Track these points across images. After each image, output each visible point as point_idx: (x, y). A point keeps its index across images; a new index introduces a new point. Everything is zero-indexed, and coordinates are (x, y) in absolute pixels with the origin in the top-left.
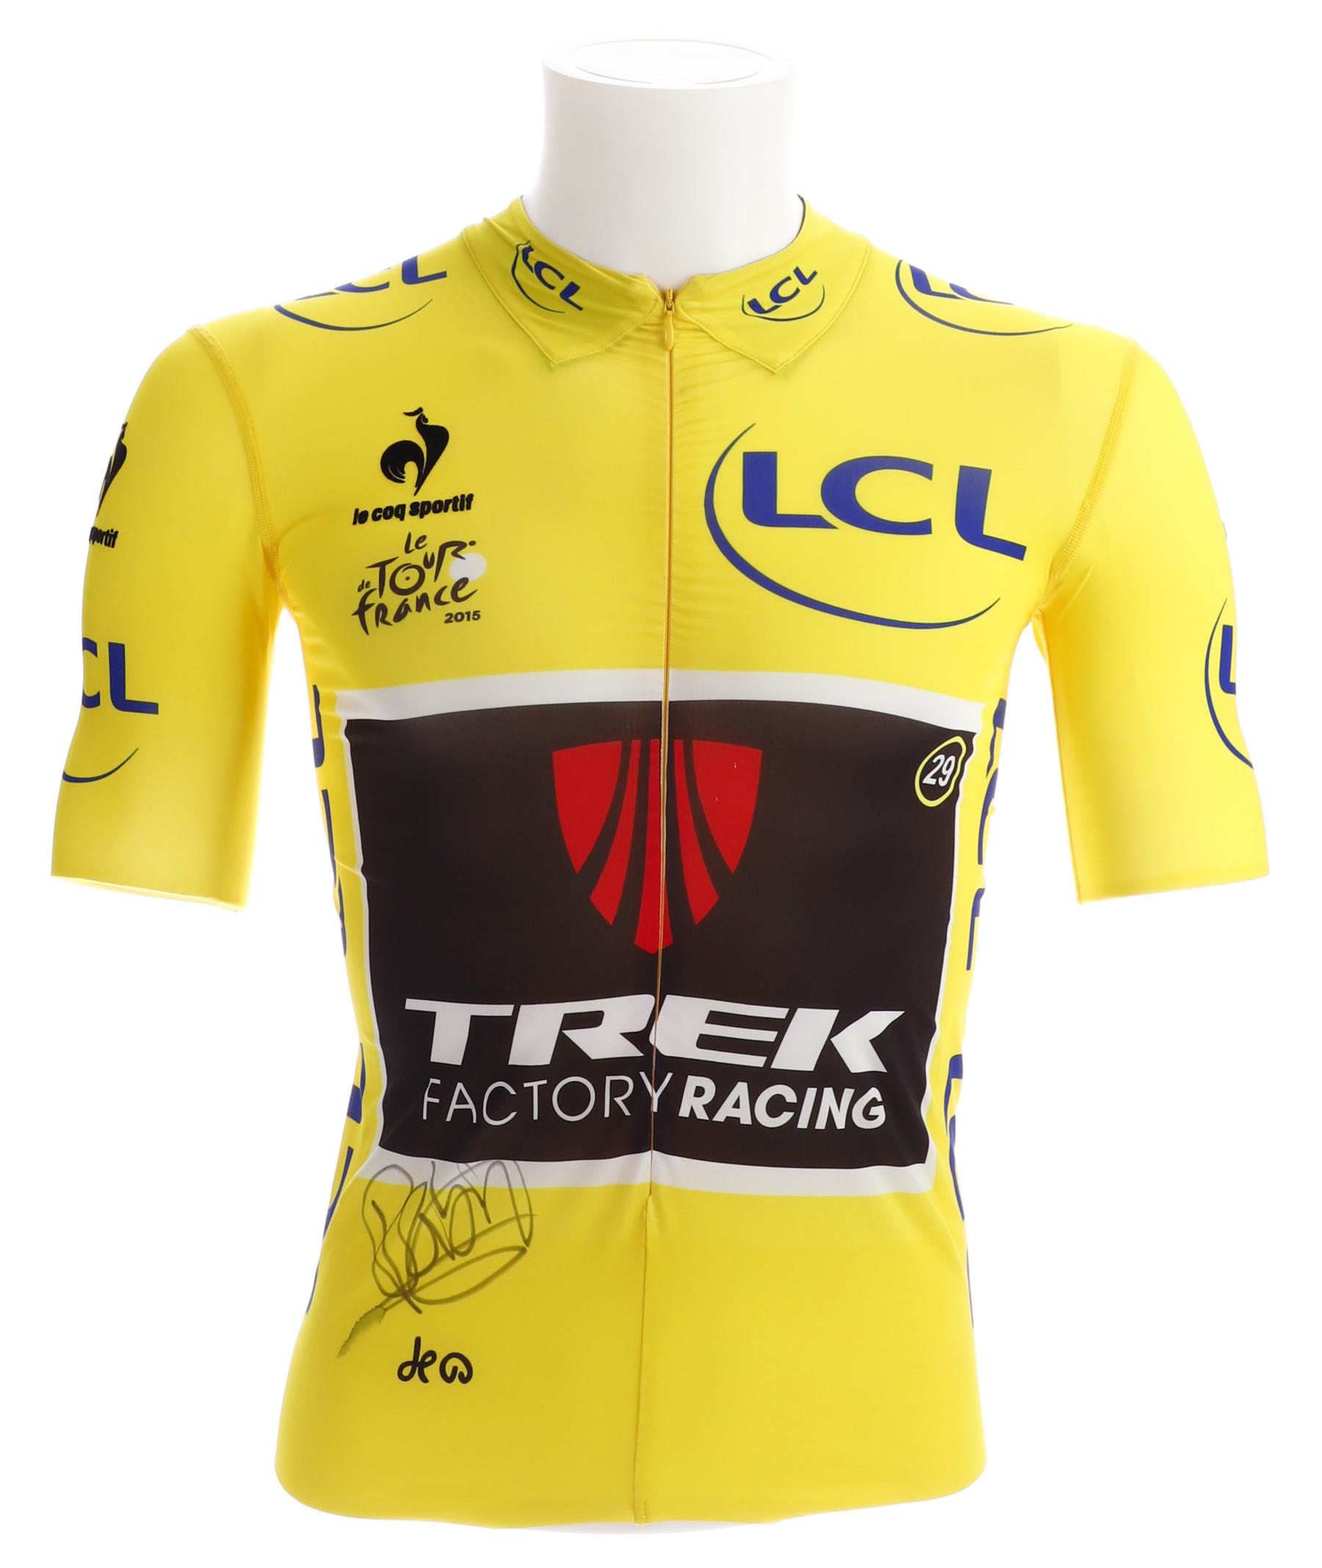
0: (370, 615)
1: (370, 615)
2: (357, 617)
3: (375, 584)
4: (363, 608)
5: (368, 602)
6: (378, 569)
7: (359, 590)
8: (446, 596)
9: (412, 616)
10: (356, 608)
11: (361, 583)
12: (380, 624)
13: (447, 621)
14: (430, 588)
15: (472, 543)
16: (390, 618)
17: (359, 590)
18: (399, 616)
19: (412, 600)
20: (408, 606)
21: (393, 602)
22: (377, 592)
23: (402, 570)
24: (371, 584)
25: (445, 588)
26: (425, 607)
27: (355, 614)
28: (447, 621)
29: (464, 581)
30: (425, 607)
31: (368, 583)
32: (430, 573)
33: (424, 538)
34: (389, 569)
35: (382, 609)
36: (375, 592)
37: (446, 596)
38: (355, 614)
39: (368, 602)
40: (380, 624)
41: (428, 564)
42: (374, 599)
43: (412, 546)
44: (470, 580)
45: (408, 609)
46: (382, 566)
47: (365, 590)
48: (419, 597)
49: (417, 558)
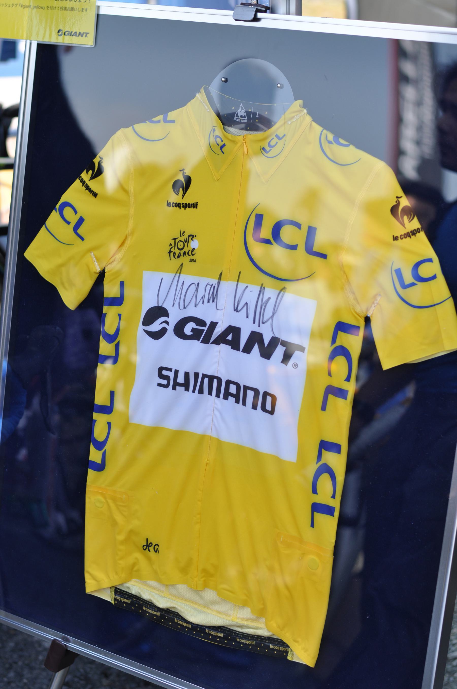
0: (172, 254)
1: (172, 254)
2: (169, 254)
3: (173, 245)
4: (170, 252)
5: (172, 250)
6: (174, 240)
7: (170, 246)
8: (190, 253)
9: (182, 257)
10: (169, 251)
11: (170, 244)
12: (174, 258)
13: (190, 261)
14: (186, 249)
15: (196, 236)
16: (176, 257)
17: (170, 246)
18: (178, 257)
19: (182, 252)
20: (180, 254)
21: (177, 252)
22: (174, 248)
23: (180, 242)
24: (172, 245)
25: (190, 250)
26: (185, 255)
27: (168, 253)
28: (190, 261)
29: (194, 249)
30: (185, 255)
31: (172, 244)
32: (186, 244)
33: (184, 232)
34: (177, 241)
35: (175, 253)
36: (173, 248)
37: (190, 253)
38: (168, 253)
39: (172, 250)
40: (174, 258)
41: (186, 242)
42: (173, 250)
43: (182, 235)
44: (195, 249)
45: (181, 255)
46: (175, 239)
47: (171, 247)
48: (183, 252)
49: (182, 239)
